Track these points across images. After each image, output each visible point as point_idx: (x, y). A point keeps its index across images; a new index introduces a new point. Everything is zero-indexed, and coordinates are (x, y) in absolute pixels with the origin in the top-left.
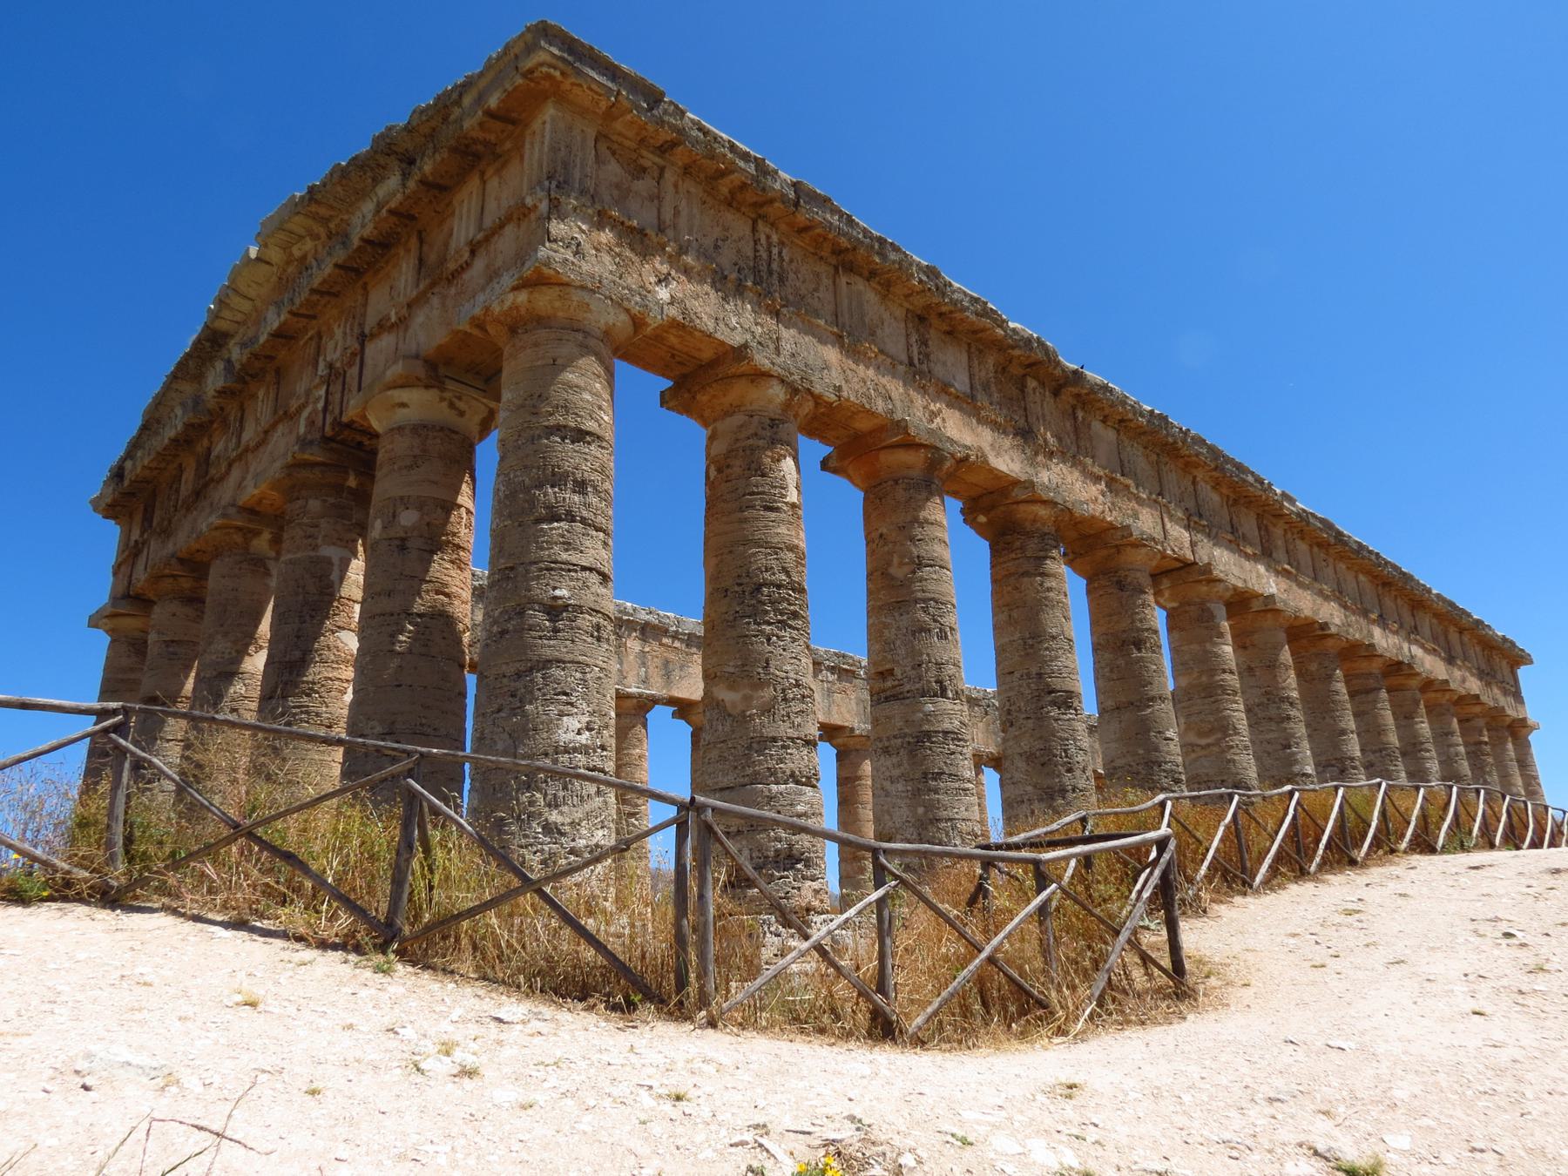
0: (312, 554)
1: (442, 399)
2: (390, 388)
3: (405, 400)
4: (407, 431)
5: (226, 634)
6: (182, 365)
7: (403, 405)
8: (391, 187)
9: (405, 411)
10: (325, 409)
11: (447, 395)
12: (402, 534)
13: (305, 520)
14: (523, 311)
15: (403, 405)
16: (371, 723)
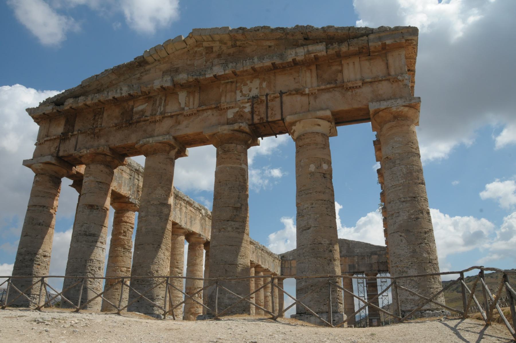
0: (240, 166)
1: (330, 127)
2: (316, 118)
3: (320, 123)
4: (320, 135)
5: (162, 187)
6: (119, 67)
7: (319, 125)
8: (319, 49)
9: (319, 127)
10: (252, 112)
11: (332, 126)
12: (324, 172)
13: (236, 152)
14: (403, 113)
15: (319, 125)
16: (324, 240)
